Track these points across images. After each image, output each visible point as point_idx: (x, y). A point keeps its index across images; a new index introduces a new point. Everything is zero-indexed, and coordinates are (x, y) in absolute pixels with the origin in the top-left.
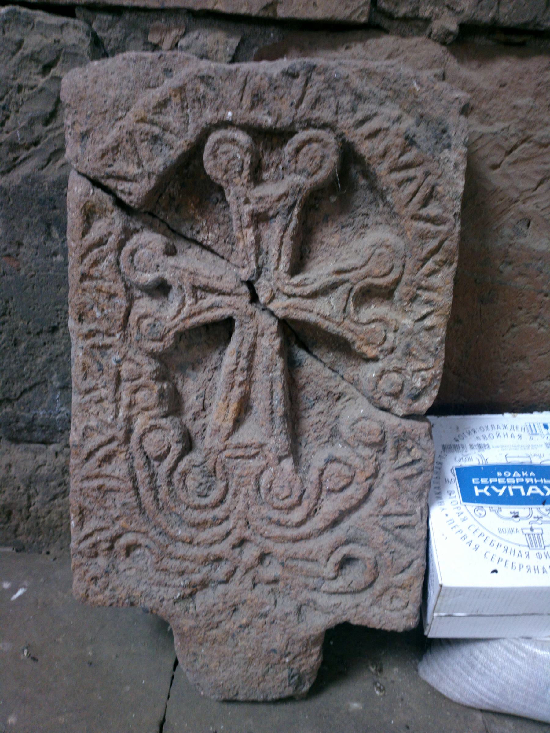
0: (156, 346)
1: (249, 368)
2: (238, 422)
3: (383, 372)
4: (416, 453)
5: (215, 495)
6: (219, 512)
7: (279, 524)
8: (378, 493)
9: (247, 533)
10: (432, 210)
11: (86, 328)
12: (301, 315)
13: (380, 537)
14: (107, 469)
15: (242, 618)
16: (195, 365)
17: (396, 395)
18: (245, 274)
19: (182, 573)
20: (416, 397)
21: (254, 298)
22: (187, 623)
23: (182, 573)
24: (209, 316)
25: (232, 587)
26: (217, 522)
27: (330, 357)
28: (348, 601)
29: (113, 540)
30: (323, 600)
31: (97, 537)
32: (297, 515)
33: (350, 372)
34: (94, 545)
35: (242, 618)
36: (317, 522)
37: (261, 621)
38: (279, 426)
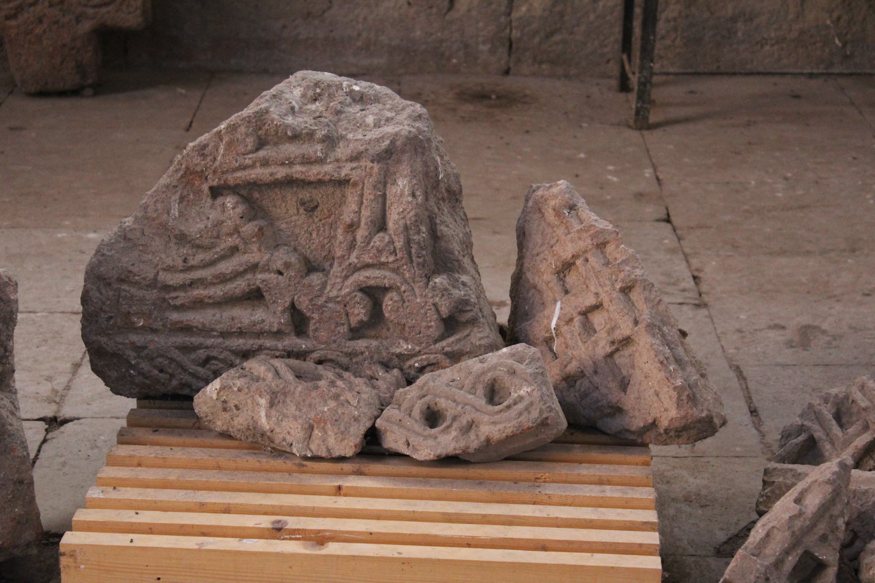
25: (39, 7)
30: (90, 11)
37: (56, 26)
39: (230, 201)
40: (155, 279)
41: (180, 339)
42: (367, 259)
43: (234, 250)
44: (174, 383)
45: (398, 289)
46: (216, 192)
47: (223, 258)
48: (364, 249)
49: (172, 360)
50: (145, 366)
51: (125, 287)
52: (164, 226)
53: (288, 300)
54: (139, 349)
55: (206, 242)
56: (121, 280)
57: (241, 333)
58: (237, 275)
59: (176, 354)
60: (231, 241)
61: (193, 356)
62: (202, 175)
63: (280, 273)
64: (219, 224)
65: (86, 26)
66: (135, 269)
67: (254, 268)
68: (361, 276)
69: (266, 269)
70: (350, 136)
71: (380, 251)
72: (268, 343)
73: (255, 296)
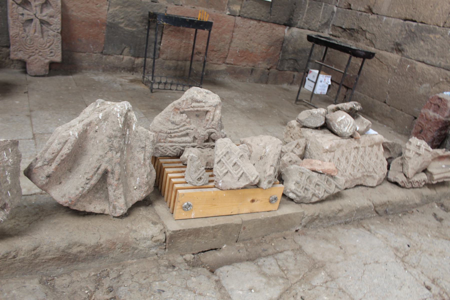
0: (22, 22)
1: (36, 26)
2: (35, 33)
3: (54, 27)
4: (59, 37)
5: (32, 43)
6: (33, 45)
7: (41, 47)
8: (55, 43)
9: (37, 48)
10: (57, 7)
11: (12, 19)
12: (42, 19)
13: (55, 48)
14: (17, 39)
15: (37, 60)
16: (28, 26)
17: (55, 29)
18: (34, 13)
19: (28, 54)
20: (58, 30)
21: (36, 16)
22: (29, 61)
23: (28, 54)
24: (29, 18)
26: (32, 47)
27: (47, 25)
28: (52, 58)
29: (18, 49)
30: (48, 58)
31: (15, 49)
32: (44, 46)
33: (49, 27)
34: (15, 50)
35: (37, 60)
36: (47, 47)
38: (40, 33)
39: (184, 115)
40: (167, 132)
41: (170, 144)
42: (210, 127)
43: (184, 125)
44: (168, 153)
45: (215, 133)
46: (182, 113)
47: (182, 127)
48: (209, 125)
49: (168, 149)
50: (163, 150)
51: (160, 133)
52: (169, 120)
53: (193, 135)
54: (161, 146)
55: (178, 124)
56: (160, 132)
57: (183, 142)
58: (184, 130)
59: (169, 147)
60: (183, 123)
61: (173, 148)
62: (179, 109)
63: (192, 130)
64: (182, 120)
65: (47, 61)
66: (162, 129)
67: (188, 129)
68: (208, 130)
69: (190, 129)
70: (209, 101)
71: (213, 125)
72: (188, 144)
73: (187, 135)
